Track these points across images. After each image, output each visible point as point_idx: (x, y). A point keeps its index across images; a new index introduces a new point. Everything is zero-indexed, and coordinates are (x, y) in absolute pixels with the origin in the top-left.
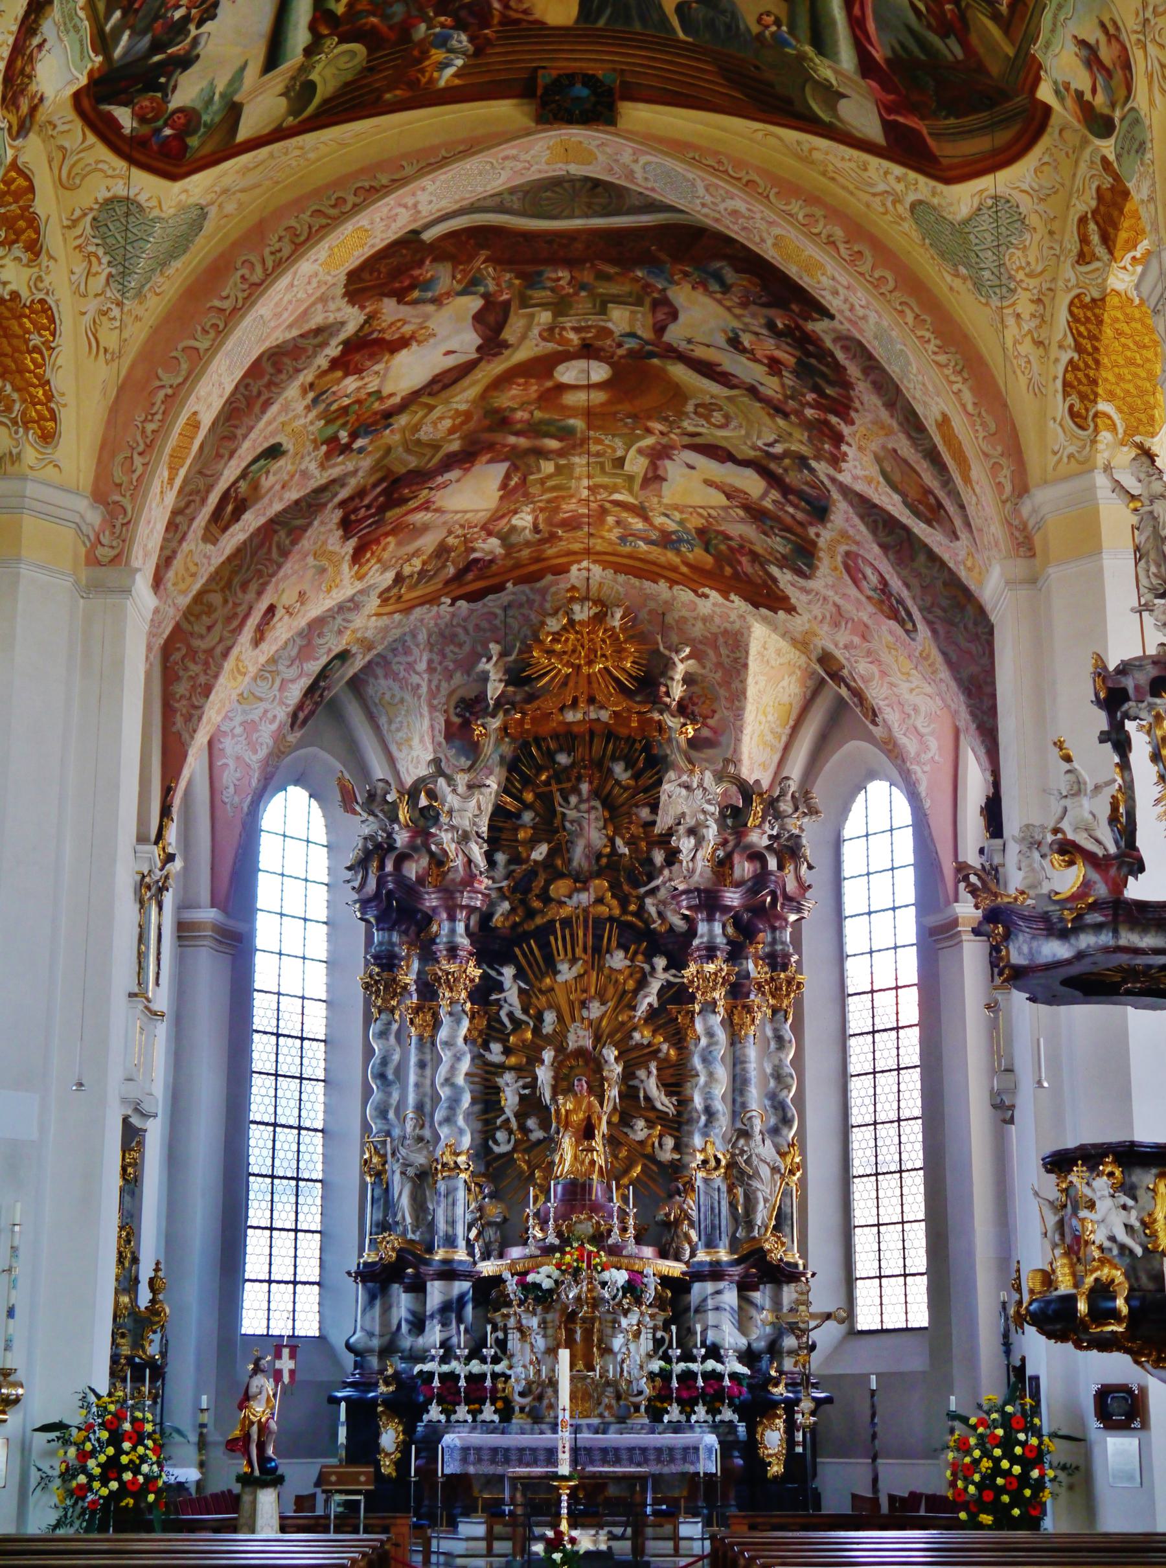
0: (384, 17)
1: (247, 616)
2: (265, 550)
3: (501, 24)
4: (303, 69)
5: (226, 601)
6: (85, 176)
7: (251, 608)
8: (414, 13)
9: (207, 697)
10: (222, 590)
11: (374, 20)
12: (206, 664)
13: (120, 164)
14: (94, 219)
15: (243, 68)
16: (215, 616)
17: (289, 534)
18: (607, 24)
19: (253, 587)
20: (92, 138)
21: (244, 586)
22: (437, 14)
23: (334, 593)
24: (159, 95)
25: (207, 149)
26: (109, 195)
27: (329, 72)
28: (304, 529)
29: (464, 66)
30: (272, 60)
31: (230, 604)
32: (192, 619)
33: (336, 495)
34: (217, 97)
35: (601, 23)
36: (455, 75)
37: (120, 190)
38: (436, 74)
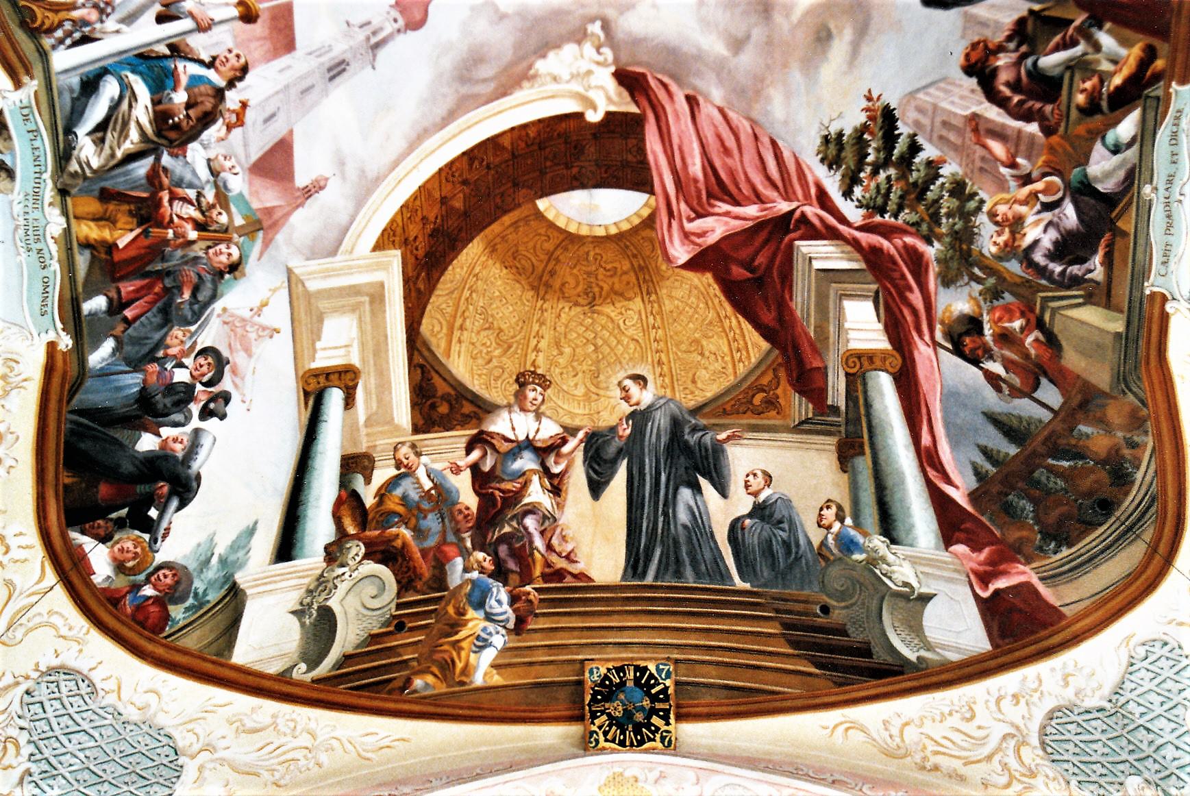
0: (419, 533)
3: (546, 577)
4: (322, 584)
6: (31, 630)
8: (451, 538)
11: (406, 533)
13: (79, 622)
14: (28, 693)
15: (251, 531)
18: (656, 578)
20: (51, 577)
22: (474, 549)
24: (147, 537)
25: (191, 641)
26: (55, 662)
27: (353, 603)
29: (505, 650)
30: (286, 550)
34: (215, 560)
35: (649, 580)
36: (495, 666)
37: (70, 658)
38: (472, 655)
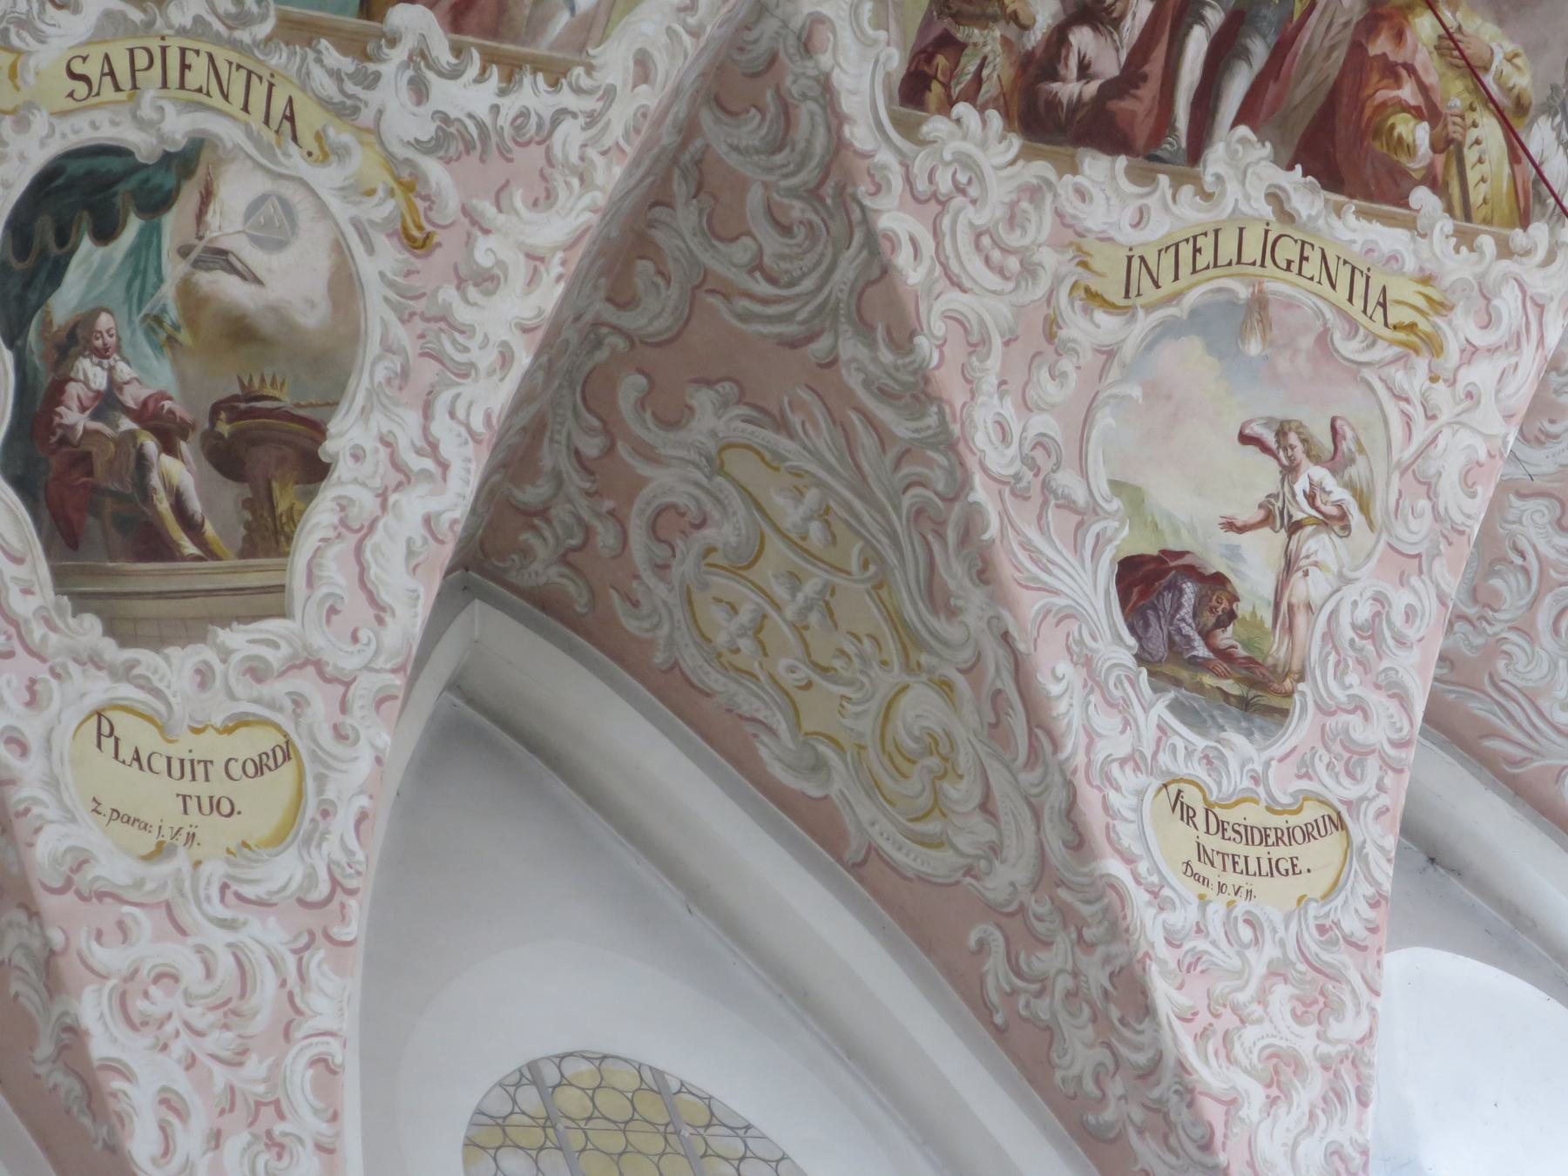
1: (1019, 668)
2: (866, 439)
5: (945, 687)
7: (1005, 636)
9: (1147, 1010)
10: (910, 667)
12: (1065, 915)
16: (964, 761)
17: (864, 328)
19: (954, 574)
21: (936, 597)
23: (1461, 328)
28: (879, 271)
31: (960, 682)
32: (932, 827)
33: (826, 89)
